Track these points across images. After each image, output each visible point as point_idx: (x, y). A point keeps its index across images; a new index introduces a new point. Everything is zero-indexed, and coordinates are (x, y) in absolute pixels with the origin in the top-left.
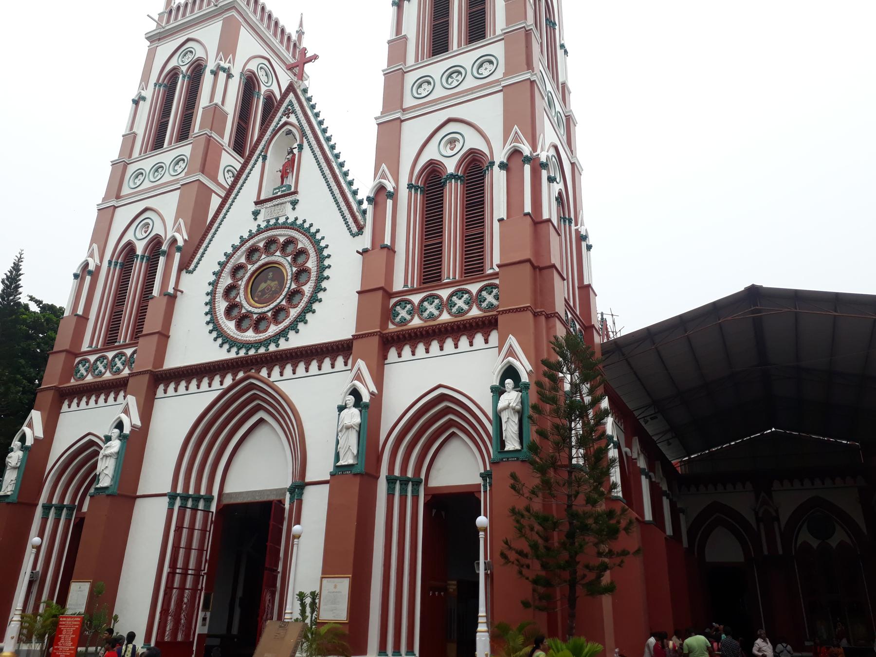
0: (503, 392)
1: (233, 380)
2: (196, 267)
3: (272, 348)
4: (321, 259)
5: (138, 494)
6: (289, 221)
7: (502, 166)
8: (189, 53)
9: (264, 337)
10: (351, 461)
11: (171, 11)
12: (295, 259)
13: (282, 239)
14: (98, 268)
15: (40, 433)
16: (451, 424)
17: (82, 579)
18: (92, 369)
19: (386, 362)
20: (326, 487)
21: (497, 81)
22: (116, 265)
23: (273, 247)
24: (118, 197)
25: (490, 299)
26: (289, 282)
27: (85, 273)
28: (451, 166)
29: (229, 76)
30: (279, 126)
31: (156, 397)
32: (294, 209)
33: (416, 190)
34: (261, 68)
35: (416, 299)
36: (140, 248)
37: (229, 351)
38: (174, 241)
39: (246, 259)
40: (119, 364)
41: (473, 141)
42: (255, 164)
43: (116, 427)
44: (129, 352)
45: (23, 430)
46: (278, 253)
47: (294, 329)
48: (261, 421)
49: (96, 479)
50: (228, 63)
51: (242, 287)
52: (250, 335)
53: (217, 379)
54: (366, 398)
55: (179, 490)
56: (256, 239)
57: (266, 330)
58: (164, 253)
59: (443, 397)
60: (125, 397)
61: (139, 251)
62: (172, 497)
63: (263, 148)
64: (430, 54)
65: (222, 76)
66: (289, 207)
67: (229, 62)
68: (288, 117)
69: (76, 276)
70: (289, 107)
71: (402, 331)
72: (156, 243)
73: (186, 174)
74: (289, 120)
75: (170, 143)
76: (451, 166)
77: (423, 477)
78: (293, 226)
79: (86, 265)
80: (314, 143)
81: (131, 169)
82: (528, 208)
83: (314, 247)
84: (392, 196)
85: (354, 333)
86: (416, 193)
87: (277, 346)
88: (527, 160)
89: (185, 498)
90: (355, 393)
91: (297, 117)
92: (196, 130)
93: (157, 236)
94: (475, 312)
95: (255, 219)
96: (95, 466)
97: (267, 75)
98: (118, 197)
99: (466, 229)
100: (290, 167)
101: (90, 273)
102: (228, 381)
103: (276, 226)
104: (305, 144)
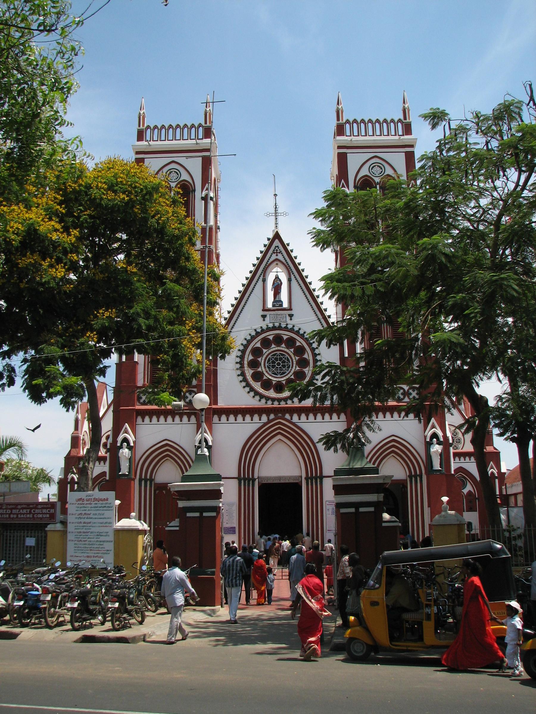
30: (271, 260)
32: (291, 319)
37: (260, 400)
52: (272, 393)
53: (256, 417)
62: (239, 479)
66: (288, 318)
68: (277, 255)
70: (277, 248)
74: (278, 257)
78: (292, 330)
95: (264, 320)
102: (264, 418)
103: (280, 328)
104: (292, 277)
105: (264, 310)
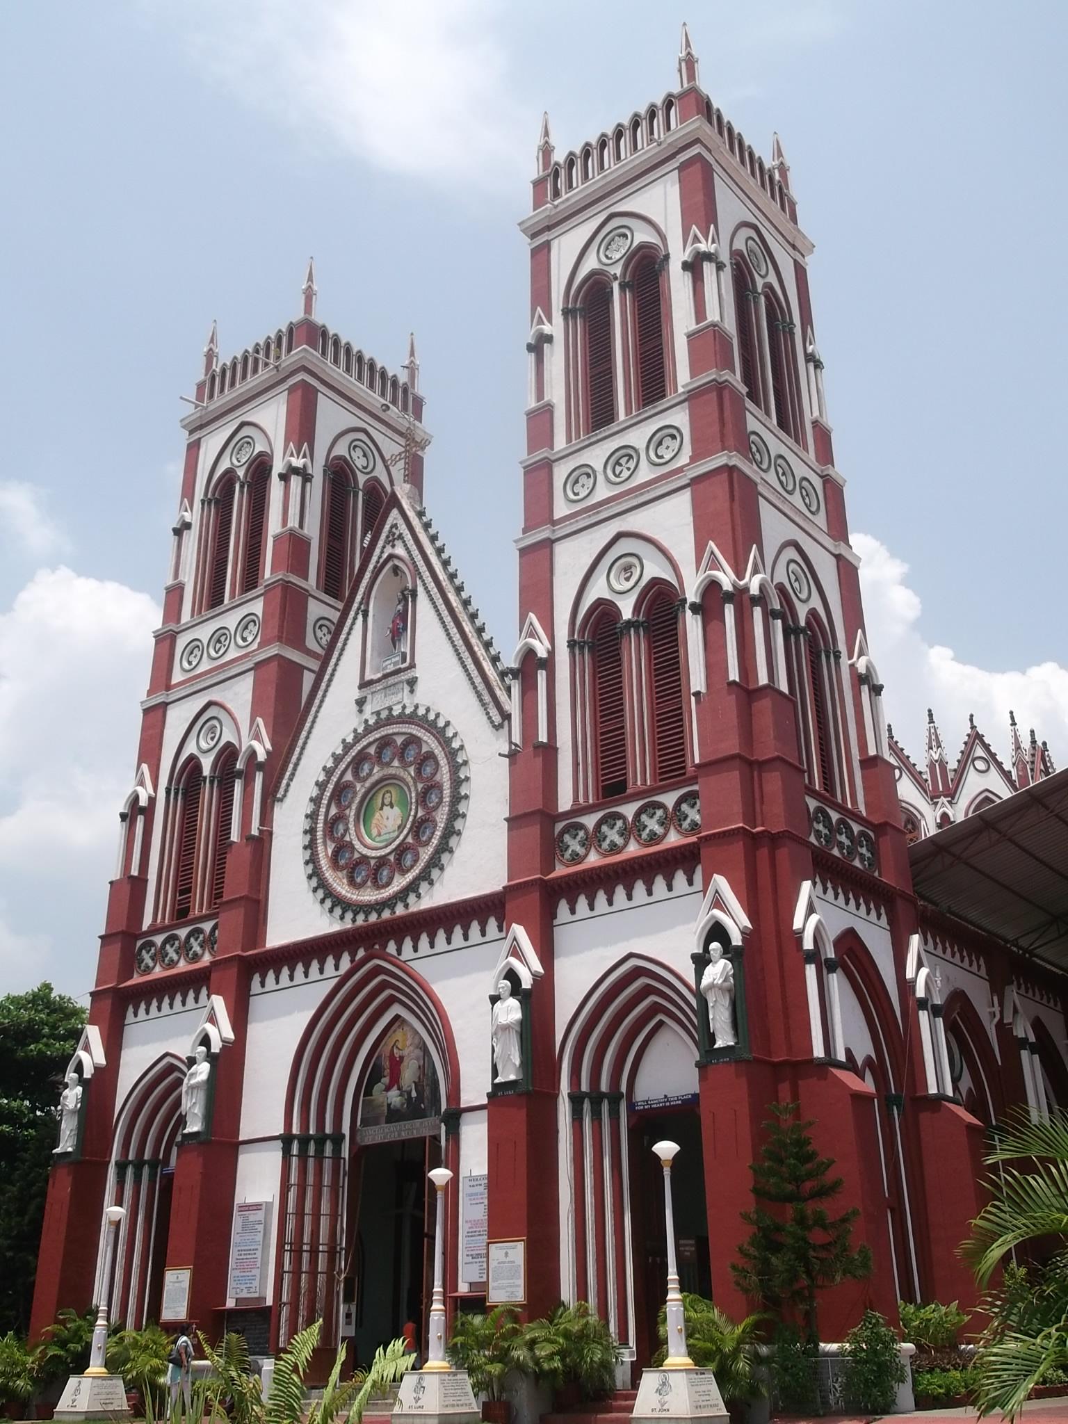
0: (709, 962)
1: (352, 961)
2: (286, 791)
3: (400, 910)
4: (455, 767)
5: (241, 1139)
6: (408, 711)
7: (695, 608)
8: (245, 445)
9: (387, 894)
10: (512, 1077)
11: (213, 378)
12: (419, 771)
13: (399, 740)
14: (152, 800)
15: (101, 1059)
16: (655, 1009)
17: (179, 1264)
18: (160, 955)
19: (556, 922)
20: (485, 1113)
21: (680, 470)
22: (176, 794)
23: (388, 753)
24: (168, 687)
25: (694, 815)
26: (414, 807)
27: (135, 812)
28: (627, 609)
29: (307, 478)
30: (381, 561)
31: (251, 993)
33: (582, 648)
34: (355, 447)
35: (590, 821)
36: (207, 764)
37: (342, 918)
38: (253, 754)
39: (353, 776)
40: (196, 948)
41: (654, 569)
42: (353, 624)
43: (201, 1044)
44: (207, 926)
45: (78, 1056)
46: (396, 763)
47: (426, 880)
48: (397, 1017)
49: (182, 1121)
50: (303, 458)
51: (351, 819)
54: (527, 983)
55: (295, 1130)
56: (364, 742)
57: (388, 884)
58: (239, 774)
59: (637, 972)
60: (209, 997)
61: (206, 771)
62: (286, 1139)
63: (363, 598)
64: (588, 429)
65: (295, 481)
67: (304, 456)
68: (393, 546)
69: (123, 817)
70: (394, 530)
71: (577, 873)
72: (228, 754)
73: (261, 646)
75: (232, 596)
76: (627, 609)
77: (623, 1089)
79: (136, 798)
80: (431, 585)
81: (182, 642)
82: (734, 675)
83: (443, 749)
84: (548, 664)
85: (505, 883)
86: (582, 654)
87: (406, 906)
88: (729, 597)
89: (304, 1140)
90: (511, 975)
91: (407, 549)
92: (267, 574)
93: (229, 744)
94: (674, 839)
95: (361, 711)
96: (178, 1102)
97: (365, 455)
98: (168, 687)
99: (658, 704)
100: (400, 627)
101: (142, 811)
103: (391, 720)
105: (364, 685)
